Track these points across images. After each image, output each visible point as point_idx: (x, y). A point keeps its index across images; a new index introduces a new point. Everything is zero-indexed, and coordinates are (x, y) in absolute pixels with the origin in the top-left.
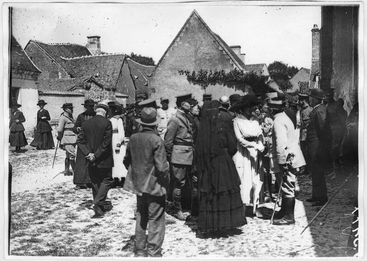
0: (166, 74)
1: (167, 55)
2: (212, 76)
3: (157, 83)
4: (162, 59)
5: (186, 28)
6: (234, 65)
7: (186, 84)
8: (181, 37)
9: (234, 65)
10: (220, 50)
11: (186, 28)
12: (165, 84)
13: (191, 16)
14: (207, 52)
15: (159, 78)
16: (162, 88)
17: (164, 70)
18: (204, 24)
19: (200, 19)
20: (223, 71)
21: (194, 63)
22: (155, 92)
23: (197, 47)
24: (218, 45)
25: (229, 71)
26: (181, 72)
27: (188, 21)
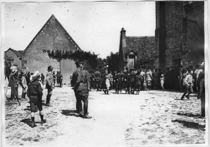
0: (35, 52)
1: (35, 40)
2: (64, 54)
3: (28, 57)
4: (31, 42)
5: (48, 25)
6: (78, 48)
7: (47, 58)
8: (44, 30)
9: (78, 48)
10: (69, 39)
11: (48, 25)
12: (34, 58)
13: (51, 18)
14: (61, 40)
15: (29, 54)
16: (31, 60)
17: (33, 50)
18: (59, 23)
19: (56, 20)
20: (71, 51)
21: (53, 46)
22: (26, 63)
23: (55, 36)
24: (68, 36)
25: (75, 51)
26: (44, 51)
27: (49, 21)
